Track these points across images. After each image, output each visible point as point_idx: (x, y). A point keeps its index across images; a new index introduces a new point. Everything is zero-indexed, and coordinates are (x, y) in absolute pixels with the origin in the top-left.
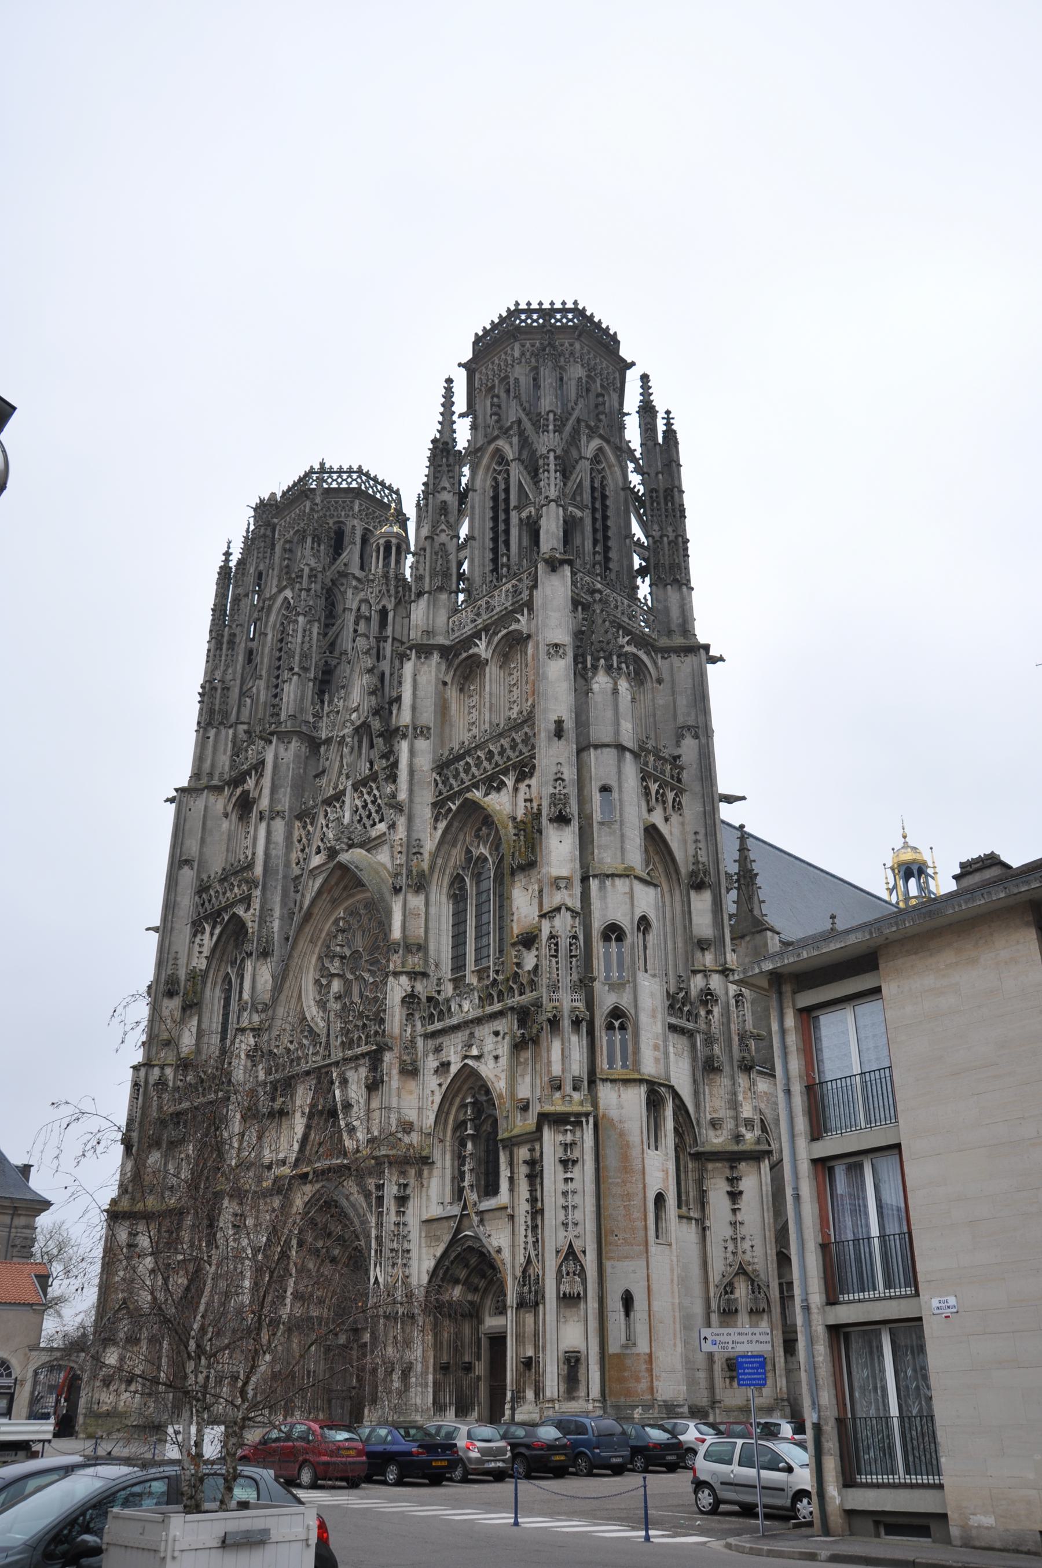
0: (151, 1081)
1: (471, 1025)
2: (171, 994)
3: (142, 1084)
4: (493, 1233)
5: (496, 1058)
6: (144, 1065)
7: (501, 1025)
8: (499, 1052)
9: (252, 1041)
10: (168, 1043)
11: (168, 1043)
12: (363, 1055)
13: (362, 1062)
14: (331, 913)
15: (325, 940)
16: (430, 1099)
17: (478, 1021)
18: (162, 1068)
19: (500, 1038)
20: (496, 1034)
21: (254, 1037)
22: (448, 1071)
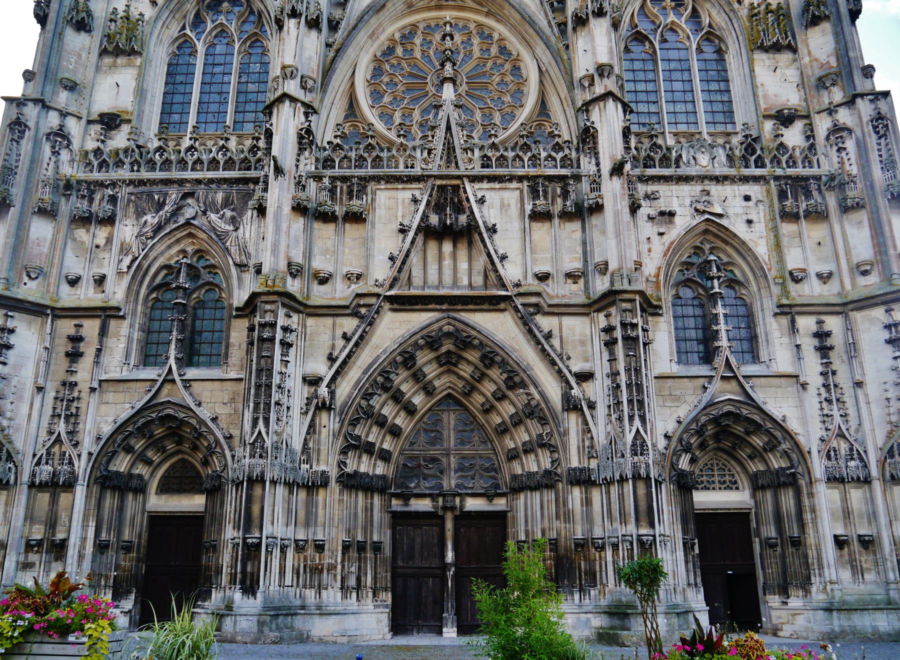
0: (44, 130)
1: (706, 182)
2: (82, 26)
3: (31, 124)
4: (768, 400)
5: (749, 222)
6: (36, 101)
7: (755, 190)
8: (750, 217)
9: (303, 119)
10: (72, 87)
11: (72, 87)
12: (520, 179)
13: (514, 185)
14: (403, 16)
15: (383, 44)
16: (647, 246)
17: (719, 179)
18: (64, 114)
19: (750, 204)
20: (747, 198)
21: (306, 114)
22: (671, 222)
